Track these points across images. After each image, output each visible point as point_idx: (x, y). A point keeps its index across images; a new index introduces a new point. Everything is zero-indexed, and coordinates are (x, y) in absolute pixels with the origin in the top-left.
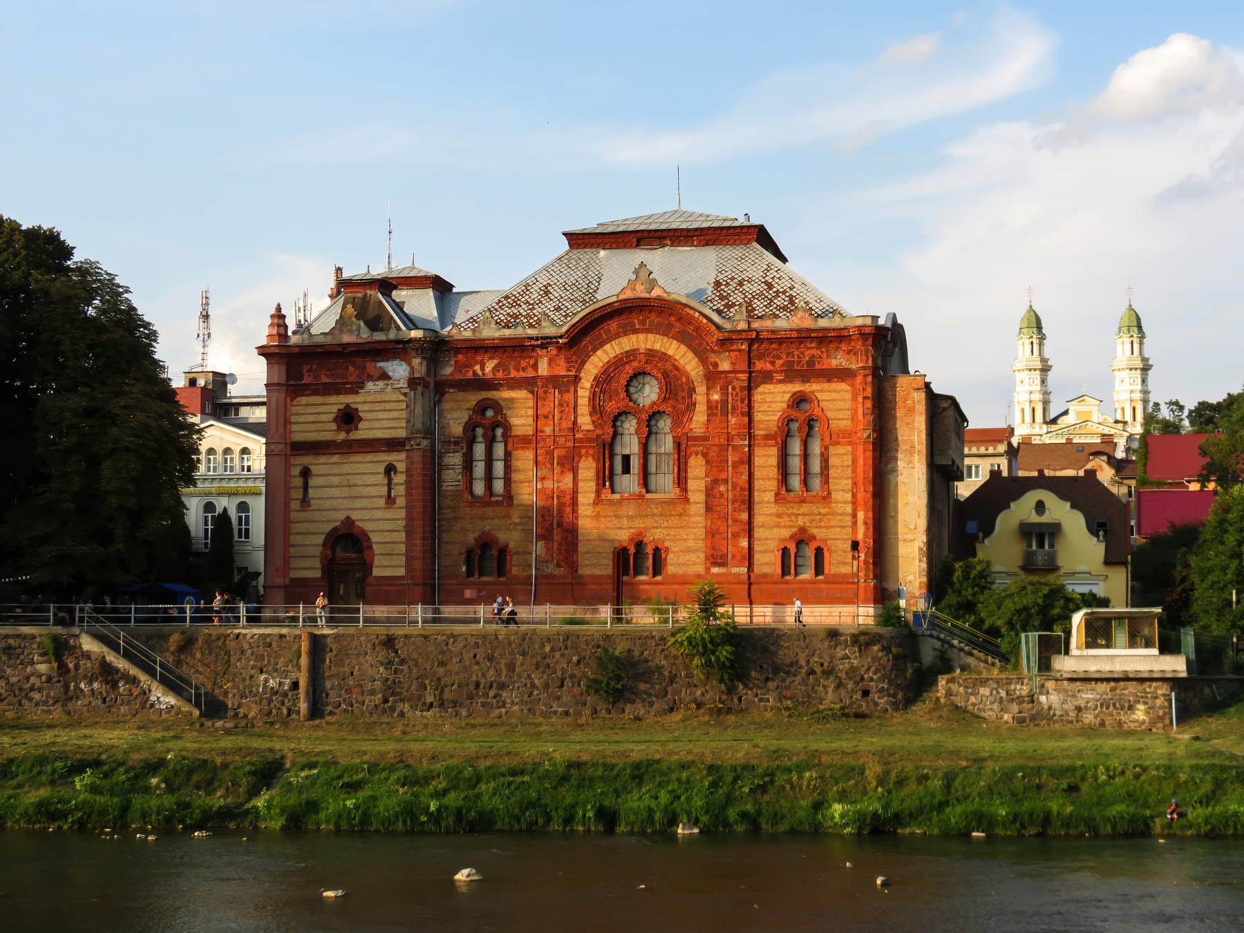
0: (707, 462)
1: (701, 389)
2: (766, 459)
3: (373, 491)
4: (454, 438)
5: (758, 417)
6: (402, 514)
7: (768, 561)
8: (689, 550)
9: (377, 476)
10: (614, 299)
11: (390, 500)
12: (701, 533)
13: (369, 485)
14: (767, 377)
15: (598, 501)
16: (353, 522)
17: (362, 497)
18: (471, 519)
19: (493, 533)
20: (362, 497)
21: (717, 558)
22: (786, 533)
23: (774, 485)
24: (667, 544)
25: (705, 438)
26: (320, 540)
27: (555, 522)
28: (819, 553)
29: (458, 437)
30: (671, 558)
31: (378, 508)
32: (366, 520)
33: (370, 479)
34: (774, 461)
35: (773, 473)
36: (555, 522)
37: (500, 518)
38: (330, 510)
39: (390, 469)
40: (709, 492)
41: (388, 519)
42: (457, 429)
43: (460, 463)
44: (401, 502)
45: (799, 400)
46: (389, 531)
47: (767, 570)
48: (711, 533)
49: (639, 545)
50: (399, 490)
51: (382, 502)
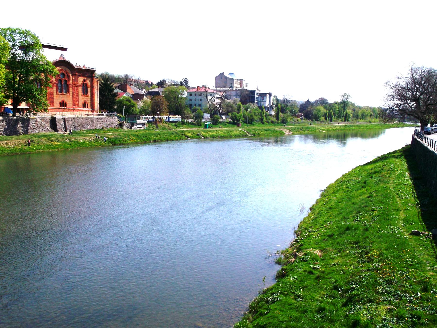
0: (73, 89)
1: (71, 77)
2: (80, 89)
5: (79, 82)
7: (81, 105)
8: (70, 103)
10: (58, 60)
12: (72, 100)
14: (79, 76)
15: (56, 94)
21: (74, 105)
22: (83, 101)
23: (81, 93)
24: (67, 102)
25: (72, 85)
28: (87, 104)
30: (68, 105)
34: (81, 90)
35: (81, 91)
40: (73, 94)
45: (85, 80)
47: (81, 107)
48: (73, 100)
49: (63, 102)
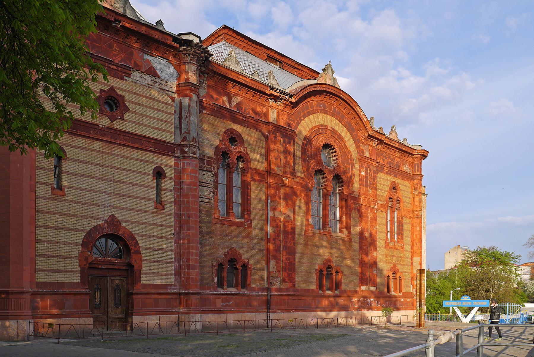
3: (140, 192)
4: (208, 157)
6: (171, 221)
9: (145, 176)
11: (159, 204)
13: (137, 185)
16: (119, 222)
17: (128, 196)
18: (220, 235)
19: (238, 249)
20: (128, 196)
26: (80, 237)
27: (282, 246)
29: (211, 158)
31: (146, 211)
32: (133, 222)
33: (136, 179)
36: (282, 246)
37: (242, 237)
38: (92, 204)
39: (159, 174)
41: (156, 225)
42: (210, 152)
43: (212, 182)
44: (170, 208)
46: (157, 237)
50: (168, 197)
51: (150, 206)
